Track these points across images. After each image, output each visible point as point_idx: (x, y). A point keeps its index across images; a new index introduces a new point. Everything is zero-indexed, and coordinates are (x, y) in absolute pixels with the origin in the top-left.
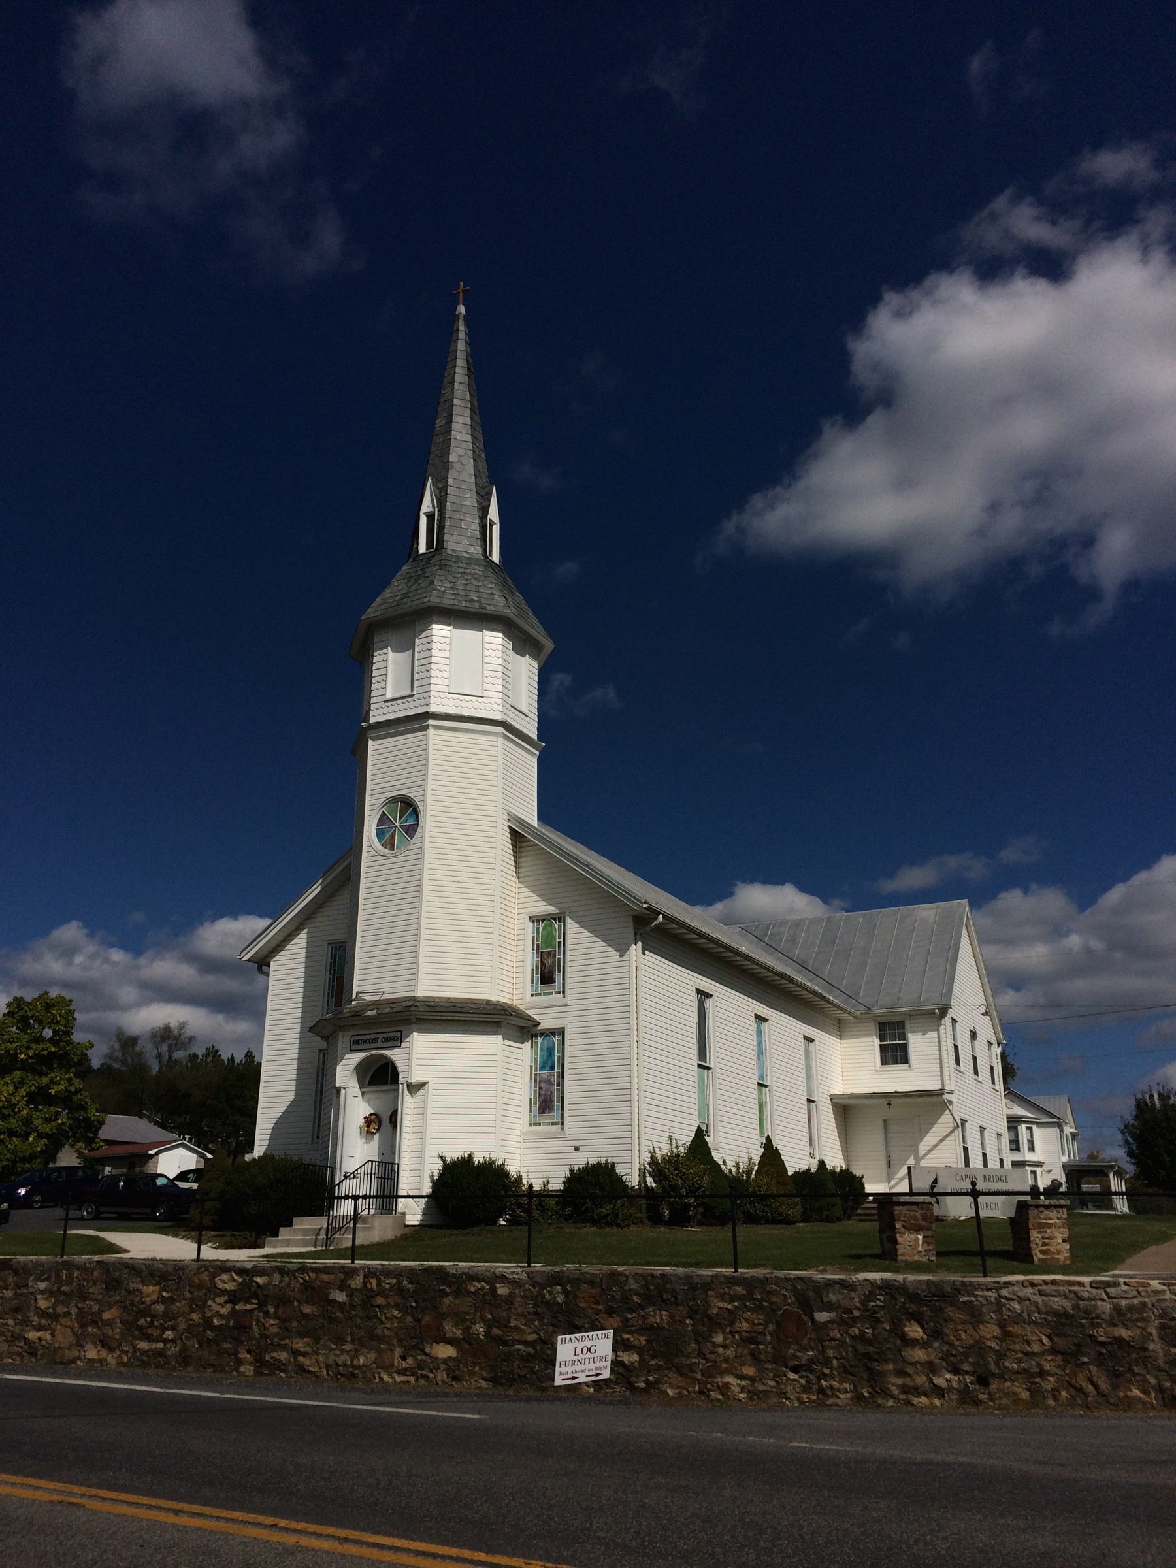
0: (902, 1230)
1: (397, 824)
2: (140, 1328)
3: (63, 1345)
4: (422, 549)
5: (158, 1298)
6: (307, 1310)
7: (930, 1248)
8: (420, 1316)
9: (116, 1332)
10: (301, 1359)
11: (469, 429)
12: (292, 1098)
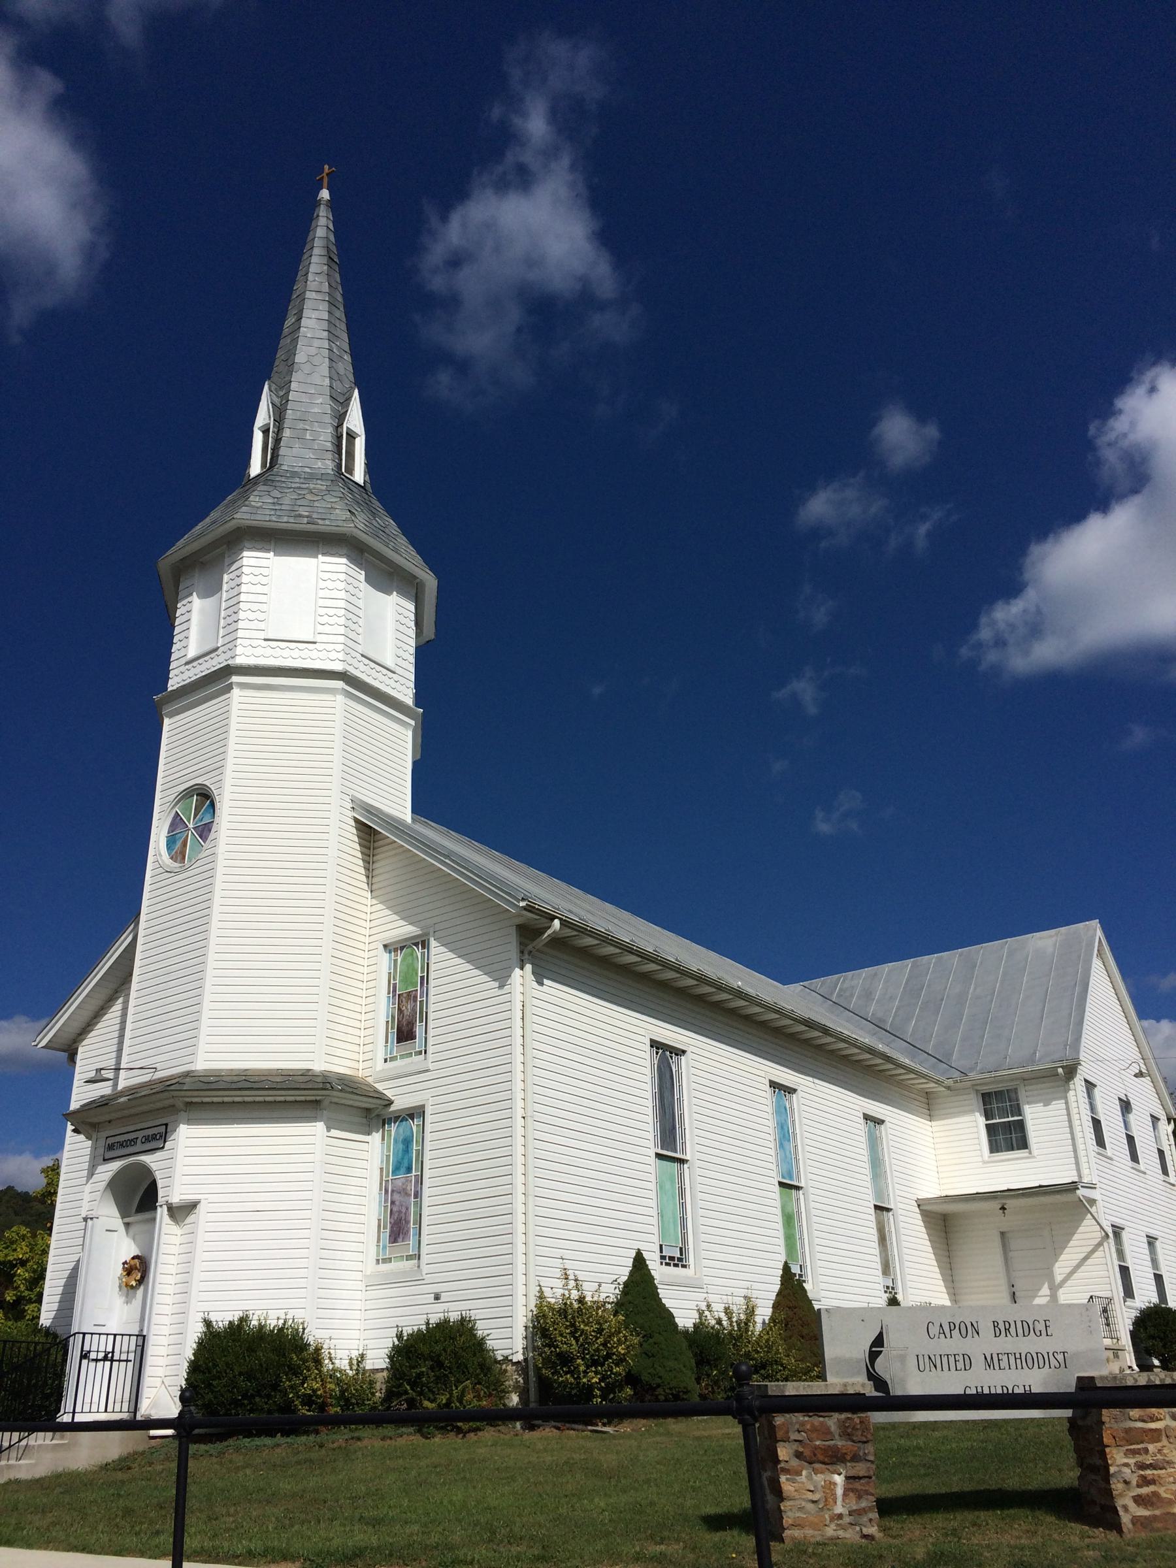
0: (795, 1463)
1: (191, 826)
7: (864, 1504)
11: (325, 325)
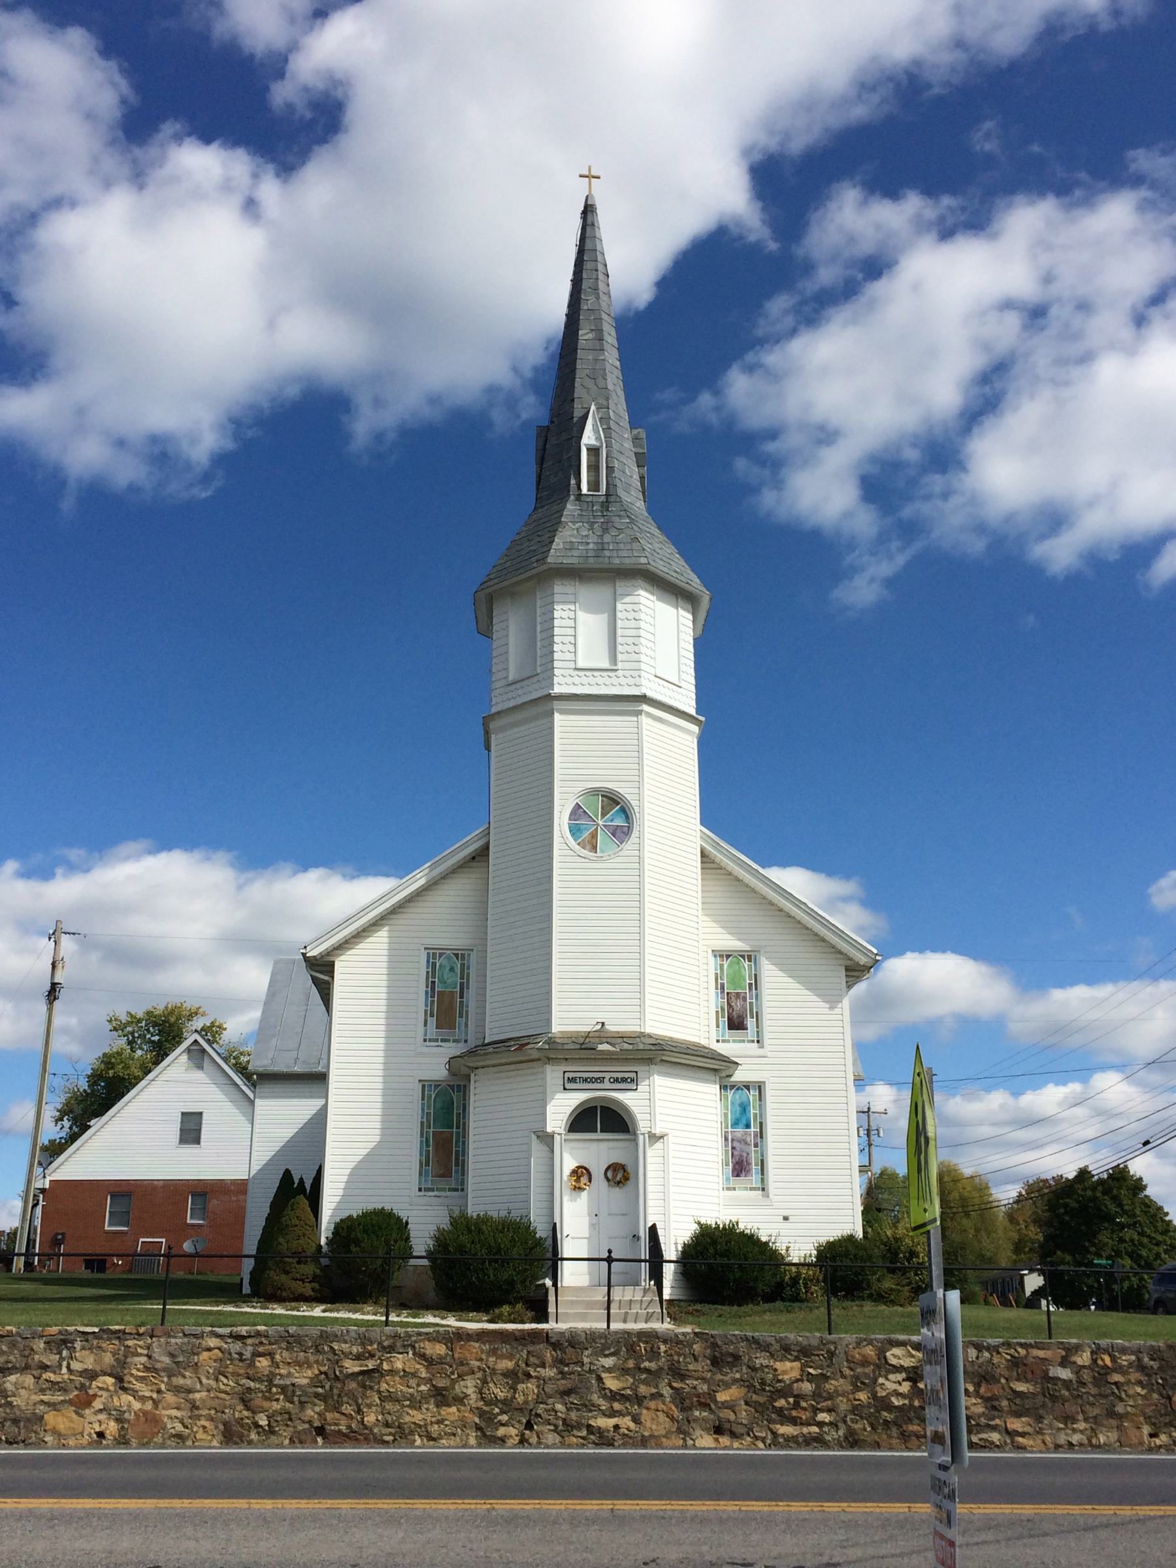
1: (600, 822)
2: (780, 1411)
3: (656, 1434)
4: (584, 490)
5: (802, 1376)
6: (1021, 1387)
8: (1170, 1393)
9: (744, 1414)
10: (1020, 1439)
12: (378, 1138)
